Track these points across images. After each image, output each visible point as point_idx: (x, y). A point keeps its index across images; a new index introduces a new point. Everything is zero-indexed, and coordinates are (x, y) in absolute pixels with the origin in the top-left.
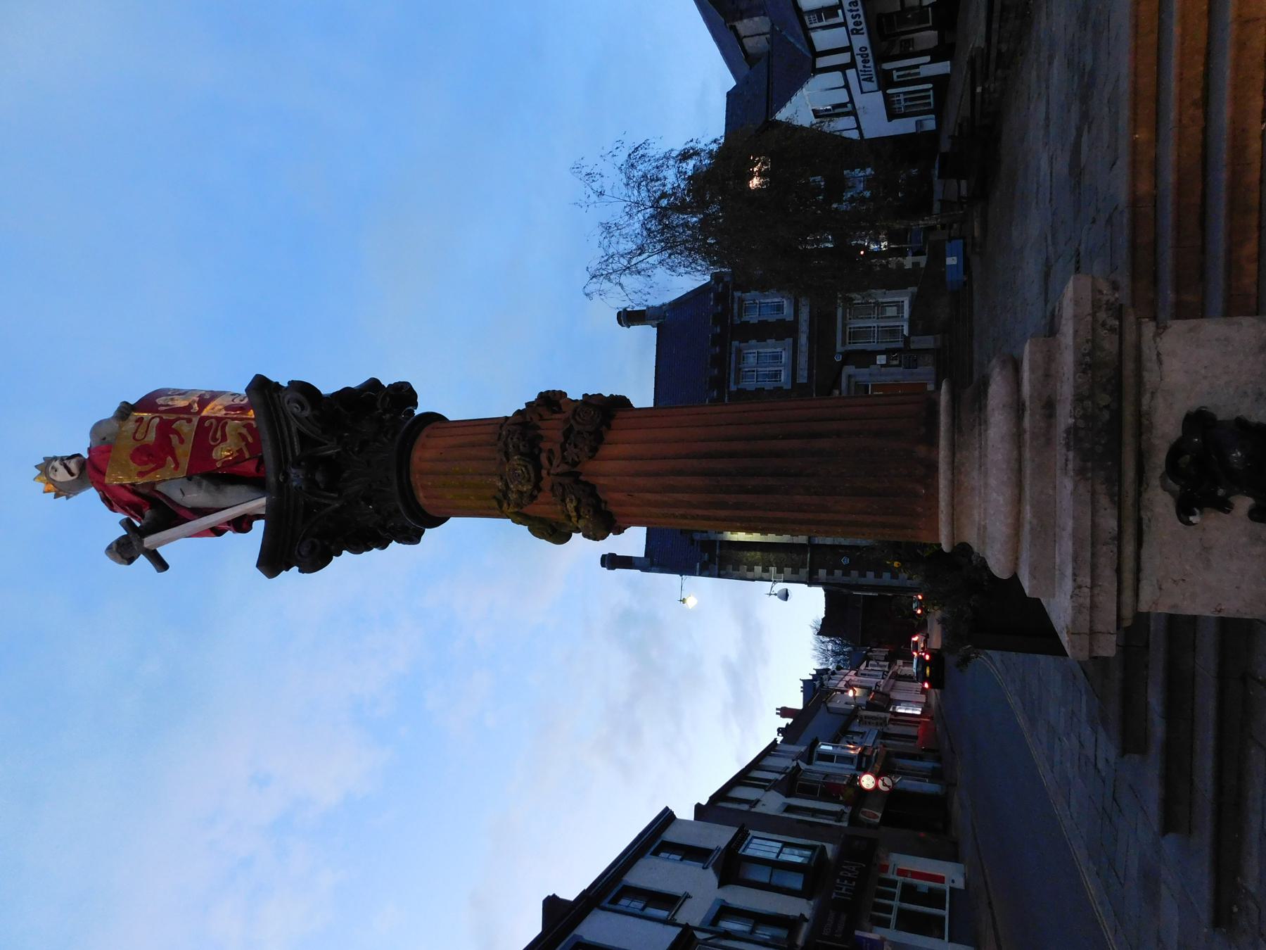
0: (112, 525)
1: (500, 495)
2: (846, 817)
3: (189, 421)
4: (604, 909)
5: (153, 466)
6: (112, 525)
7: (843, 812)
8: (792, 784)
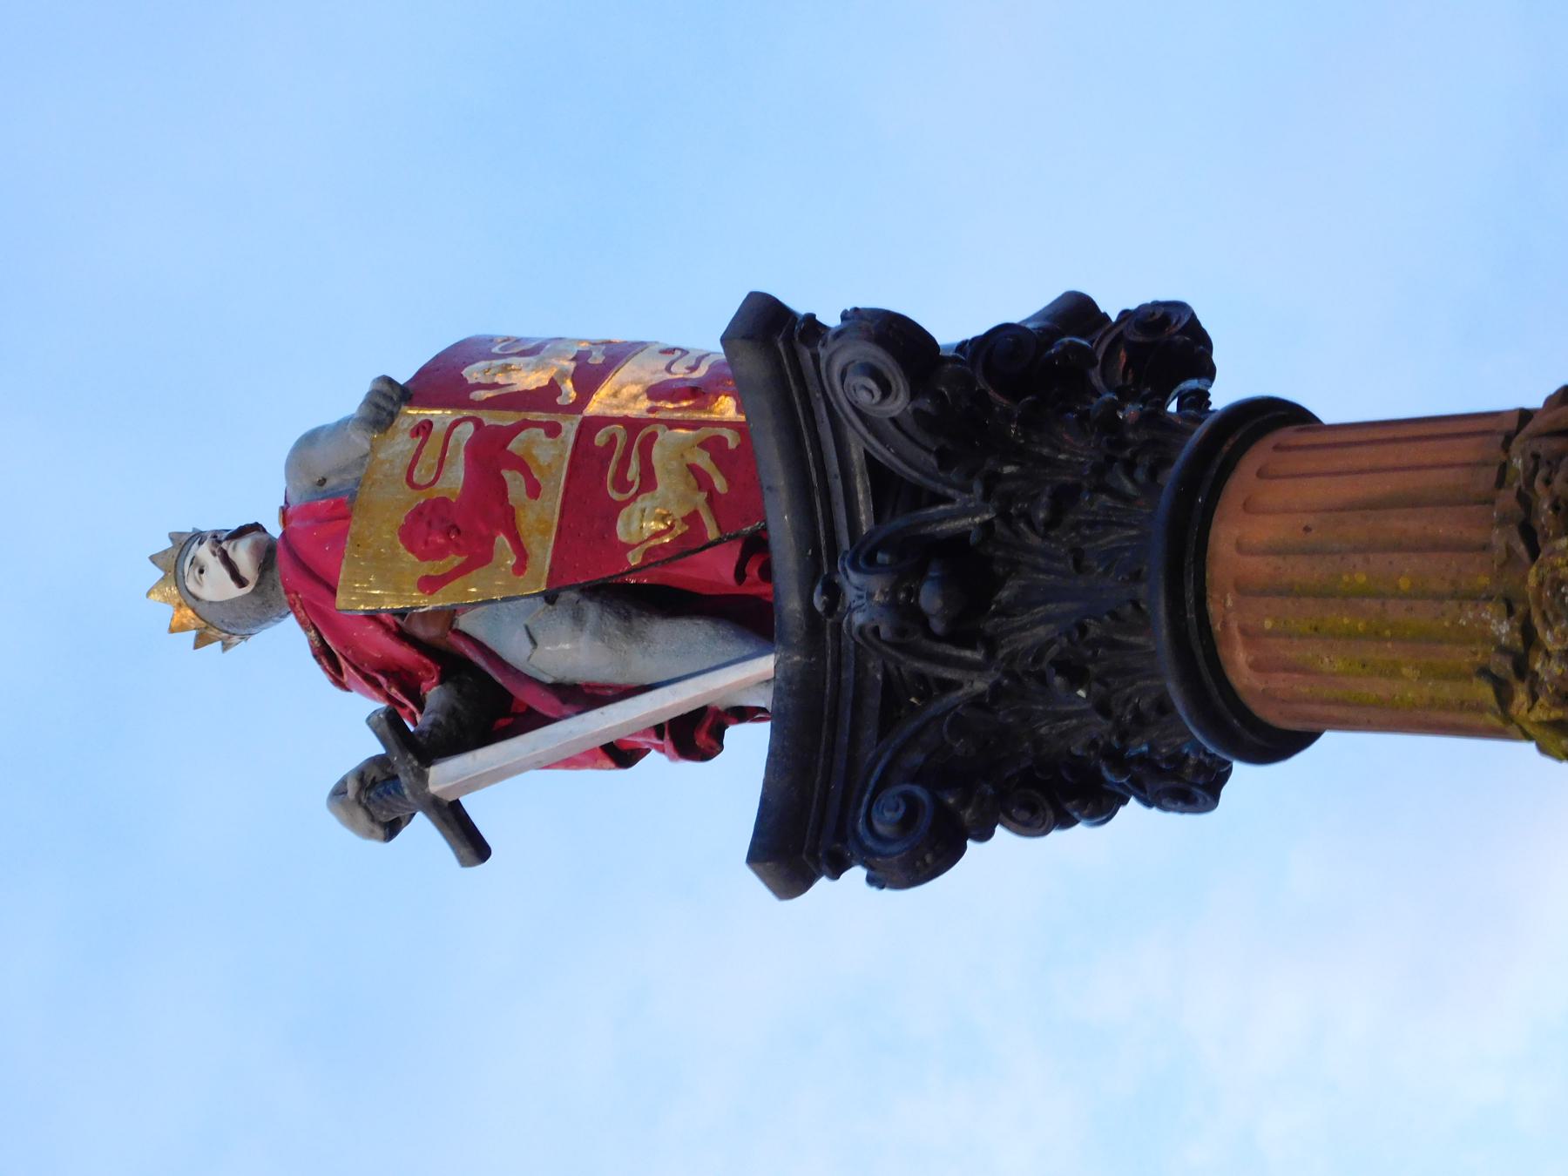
1: (1502, 666)
3: (553, 430)
5: (455, 560)
6: (348, 728)
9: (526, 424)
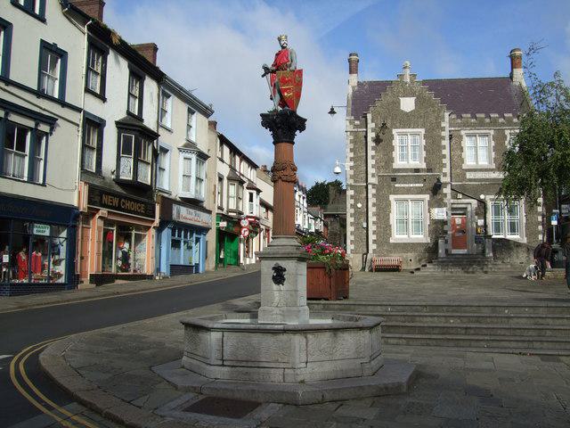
0: (270, 66)
2: (220, 211)
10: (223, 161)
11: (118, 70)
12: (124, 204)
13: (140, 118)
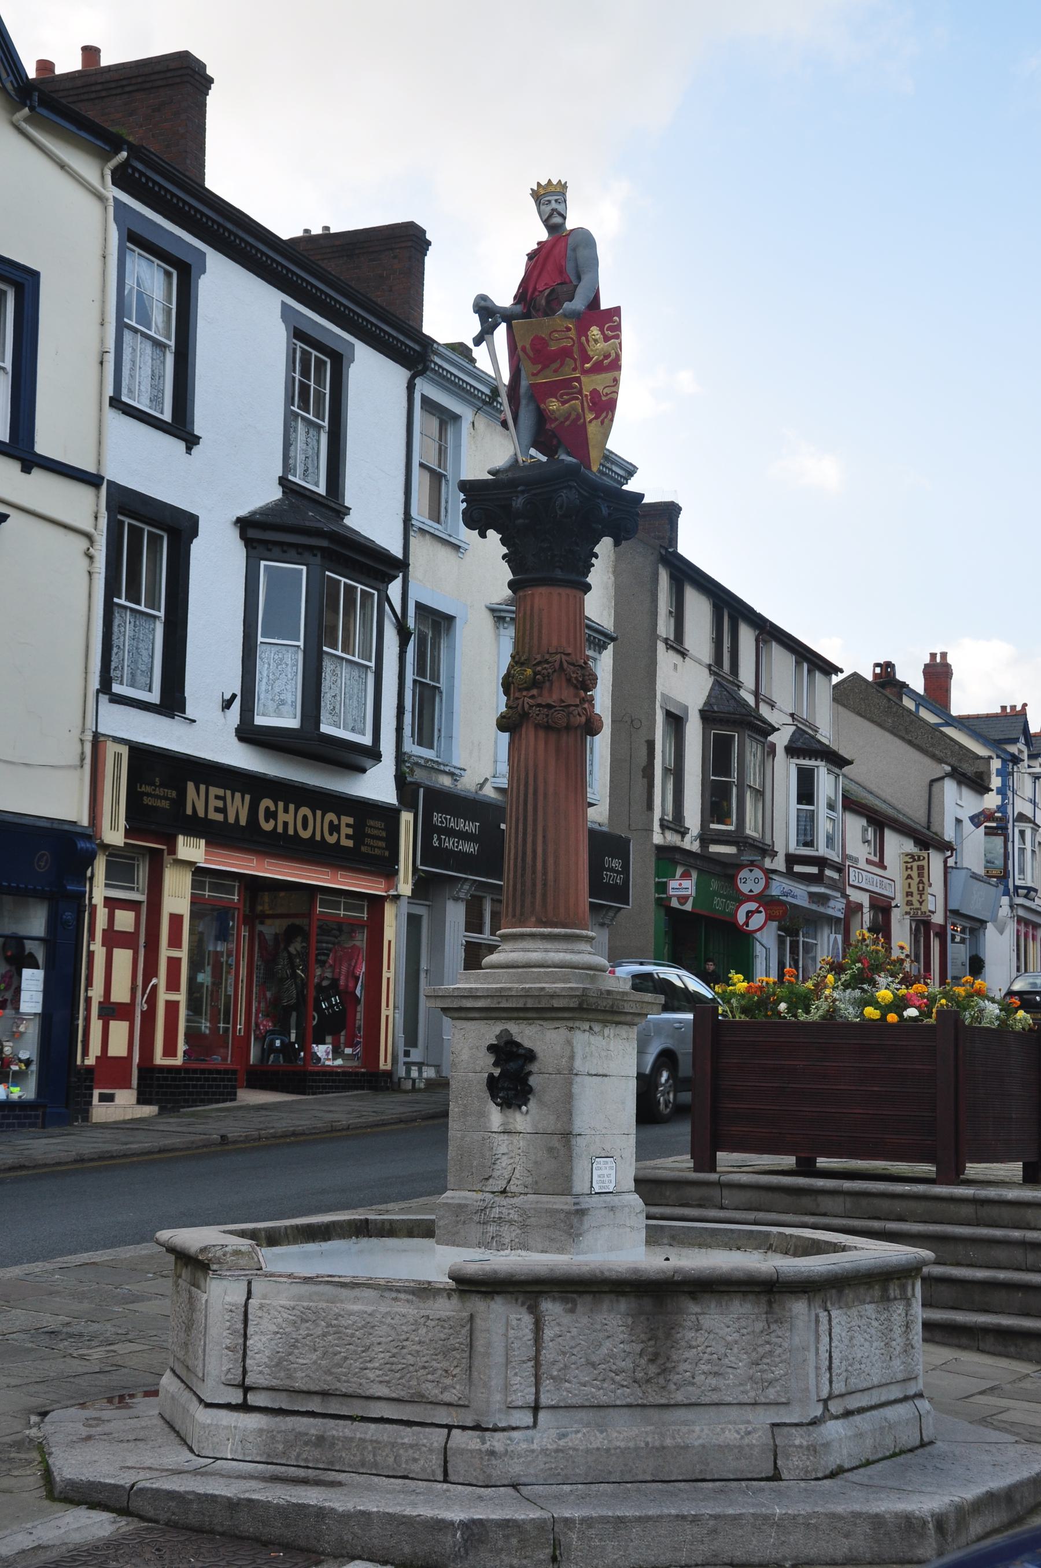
2: (672, 838)
3: (574, 369)
4: (411, 388)
7: (683, 833)
8: (732, 721)
9: (575, 360)
10: (683, 654)
11: (243, 322)
12: (270, 815)
13: (333, 503)
